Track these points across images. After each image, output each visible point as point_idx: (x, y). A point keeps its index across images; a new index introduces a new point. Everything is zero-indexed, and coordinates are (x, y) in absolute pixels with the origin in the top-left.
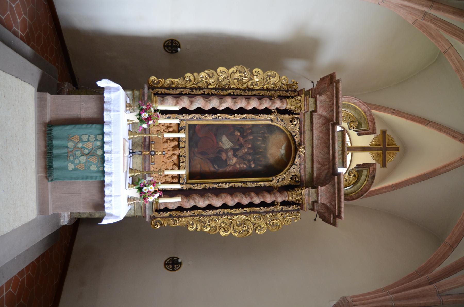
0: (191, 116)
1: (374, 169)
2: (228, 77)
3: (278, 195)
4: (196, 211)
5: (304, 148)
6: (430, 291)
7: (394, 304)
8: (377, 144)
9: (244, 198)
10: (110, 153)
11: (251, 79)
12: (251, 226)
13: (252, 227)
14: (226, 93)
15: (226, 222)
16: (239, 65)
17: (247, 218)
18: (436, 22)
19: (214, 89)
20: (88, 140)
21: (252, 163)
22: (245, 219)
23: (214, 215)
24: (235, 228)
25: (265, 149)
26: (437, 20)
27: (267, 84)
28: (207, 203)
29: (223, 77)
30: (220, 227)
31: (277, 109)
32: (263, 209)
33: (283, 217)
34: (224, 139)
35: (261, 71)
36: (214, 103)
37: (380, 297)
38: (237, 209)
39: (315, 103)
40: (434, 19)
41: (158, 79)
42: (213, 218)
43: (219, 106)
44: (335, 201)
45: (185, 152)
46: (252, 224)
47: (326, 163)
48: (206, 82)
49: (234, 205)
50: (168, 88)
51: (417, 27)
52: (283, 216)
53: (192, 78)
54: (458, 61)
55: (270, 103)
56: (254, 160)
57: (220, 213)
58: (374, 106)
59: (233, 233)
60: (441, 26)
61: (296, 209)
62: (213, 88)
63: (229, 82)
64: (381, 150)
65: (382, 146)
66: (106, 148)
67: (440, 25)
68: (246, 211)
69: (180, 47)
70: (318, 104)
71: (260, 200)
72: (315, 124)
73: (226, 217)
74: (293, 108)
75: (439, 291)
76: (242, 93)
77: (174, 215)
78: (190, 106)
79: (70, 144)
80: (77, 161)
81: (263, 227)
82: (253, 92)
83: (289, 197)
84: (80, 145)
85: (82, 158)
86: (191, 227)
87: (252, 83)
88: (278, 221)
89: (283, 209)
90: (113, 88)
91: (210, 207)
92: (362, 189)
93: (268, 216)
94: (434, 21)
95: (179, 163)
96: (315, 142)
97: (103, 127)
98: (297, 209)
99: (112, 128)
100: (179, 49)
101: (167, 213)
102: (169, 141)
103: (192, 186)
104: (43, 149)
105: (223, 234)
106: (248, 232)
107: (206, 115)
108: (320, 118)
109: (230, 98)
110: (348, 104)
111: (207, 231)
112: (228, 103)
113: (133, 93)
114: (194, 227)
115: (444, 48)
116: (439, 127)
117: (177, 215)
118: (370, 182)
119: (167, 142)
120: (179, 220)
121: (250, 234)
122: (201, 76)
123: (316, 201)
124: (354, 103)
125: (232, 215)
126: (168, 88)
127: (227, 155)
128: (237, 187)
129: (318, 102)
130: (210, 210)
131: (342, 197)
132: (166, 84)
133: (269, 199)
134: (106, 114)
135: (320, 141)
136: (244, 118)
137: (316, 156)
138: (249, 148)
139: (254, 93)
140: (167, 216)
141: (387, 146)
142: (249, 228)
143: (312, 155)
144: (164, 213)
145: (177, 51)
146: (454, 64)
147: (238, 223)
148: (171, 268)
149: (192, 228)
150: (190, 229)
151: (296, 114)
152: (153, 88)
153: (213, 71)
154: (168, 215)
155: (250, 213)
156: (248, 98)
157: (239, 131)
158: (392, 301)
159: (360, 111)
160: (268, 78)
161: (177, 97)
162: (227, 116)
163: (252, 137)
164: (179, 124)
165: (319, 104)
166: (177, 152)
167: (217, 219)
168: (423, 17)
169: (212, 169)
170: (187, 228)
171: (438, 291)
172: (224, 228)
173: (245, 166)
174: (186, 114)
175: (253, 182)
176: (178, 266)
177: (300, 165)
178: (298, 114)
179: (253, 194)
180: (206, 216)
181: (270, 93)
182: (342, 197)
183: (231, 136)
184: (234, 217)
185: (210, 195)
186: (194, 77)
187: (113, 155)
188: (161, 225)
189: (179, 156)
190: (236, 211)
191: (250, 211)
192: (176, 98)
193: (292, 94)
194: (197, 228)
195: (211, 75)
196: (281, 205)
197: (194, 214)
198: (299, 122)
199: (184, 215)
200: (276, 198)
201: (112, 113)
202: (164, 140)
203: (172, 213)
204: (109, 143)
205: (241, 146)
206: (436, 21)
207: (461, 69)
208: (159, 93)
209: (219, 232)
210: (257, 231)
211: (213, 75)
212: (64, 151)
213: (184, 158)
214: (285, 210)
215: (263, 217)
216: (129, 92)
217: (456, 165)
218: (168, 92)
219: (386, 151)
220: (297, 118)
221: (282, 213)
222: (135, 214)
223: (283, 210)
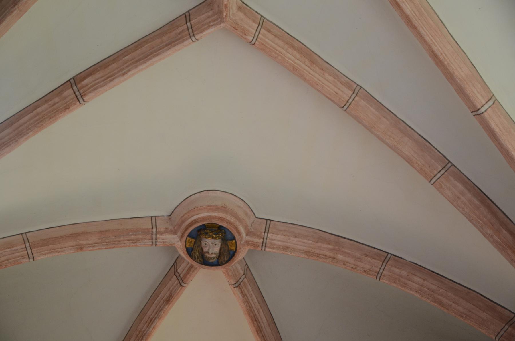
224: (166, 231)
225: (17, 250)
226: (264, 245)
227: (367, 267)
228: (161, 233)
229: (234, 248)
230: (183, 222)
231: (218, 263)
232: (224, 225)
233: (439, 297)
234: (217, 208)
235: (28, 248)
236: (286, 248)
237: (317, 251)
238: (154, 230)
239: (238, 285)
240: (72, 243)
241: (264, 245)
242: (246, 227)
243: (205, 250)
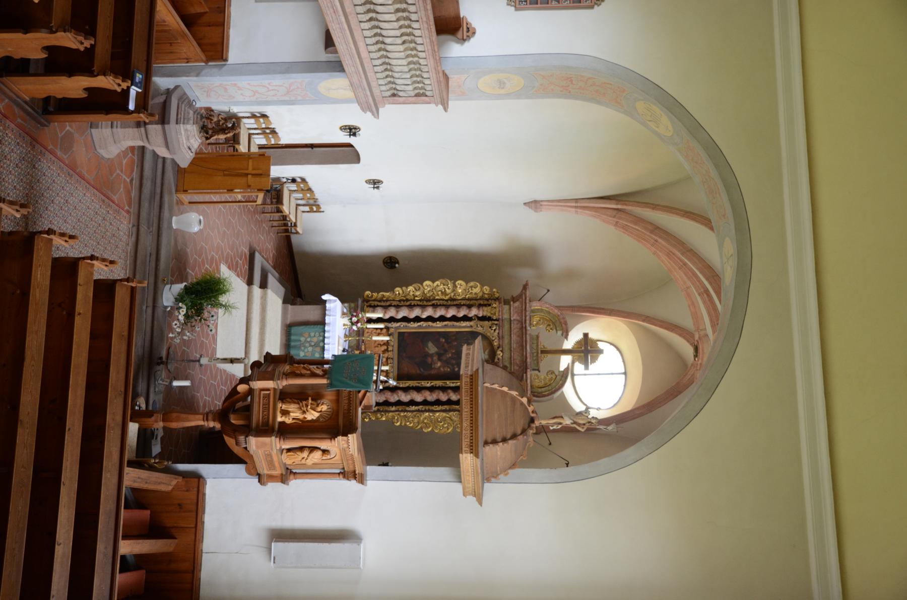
0: (399, 324)
2: (433, 289)
5: (502, 351)
10: (329, 344)
11: (454, 291)
14: (430, 304)
16: (443, 278)
19: (419, 300)
20: (315, 336)
21: (455, 366)
22: (446, 417)
27: (470, 294)
29: (429, 289)
34: (430, 345)
35: (463, 283)
36: (416, 312)
39: (510, 309)
41: (372, 293)
47: (522, 365)
49: (433, 400)
50: (380, 301)
53: (401, 292)
55: (468, 311)
63: (434, 294)
66: (326, 341)
69: (398, 263)
70: (512, 310)
73: (427, 414)
74: (489, 315)
76: (445, 303)
78: (396, 315)
79: (302, 339)
80: (306, 350)
82: (454, 302)
84: (309, 340)
85: (309, 348)
87: (455, 294)
97: (325, 326)
99: (331, 328)
100: (397, 265)
102: (379, 346)
104: (284, 341)
105: (425, 431)
106: (448, 429)
107: (412, 323)
108: (517, 324)
110: (541, 309)
112: (429, 312)
113: (350, 305)
119: (378, 347)
122: (409, 290)
124: (547, 308)
128: (437, 386)
129: (512, 308)
132: (379, 297)
134: (327, 318)
135: (518, 345)
136: (445, 325)
138: (453, 353)
139: (455, 303)
143: (511, 358)
145: (395, 267)
149: (397, 422)
152: (368, 301)
153: (419, 285)
155: (450, 411)
157: (444, 337)
160: (470, 289)
162: (430, 323)
163: (456, 343)
165: (513, 310)
166: (386, 355)
169: (418, 372)
170: (393, 423)
173: (449, 370)
174: (394, 322)
179: (450, 391)
180: (410, 411)
185: (411, 391)
186: (403, 291)
187: (330, 346)
192: (385, 308)
195: (417, 288)
198: (498, 328)
201: (331, 317)
202: (376, 345)
204: (329, 338)
205: (446, 351)
208: (372, 305)
211: (420, 288)
212: (298, 343)
213: (391, 360)
216: (346, 305)
218: (379, 304)
220: (496, 324)
224: (699, 335)
234: (703, 350)
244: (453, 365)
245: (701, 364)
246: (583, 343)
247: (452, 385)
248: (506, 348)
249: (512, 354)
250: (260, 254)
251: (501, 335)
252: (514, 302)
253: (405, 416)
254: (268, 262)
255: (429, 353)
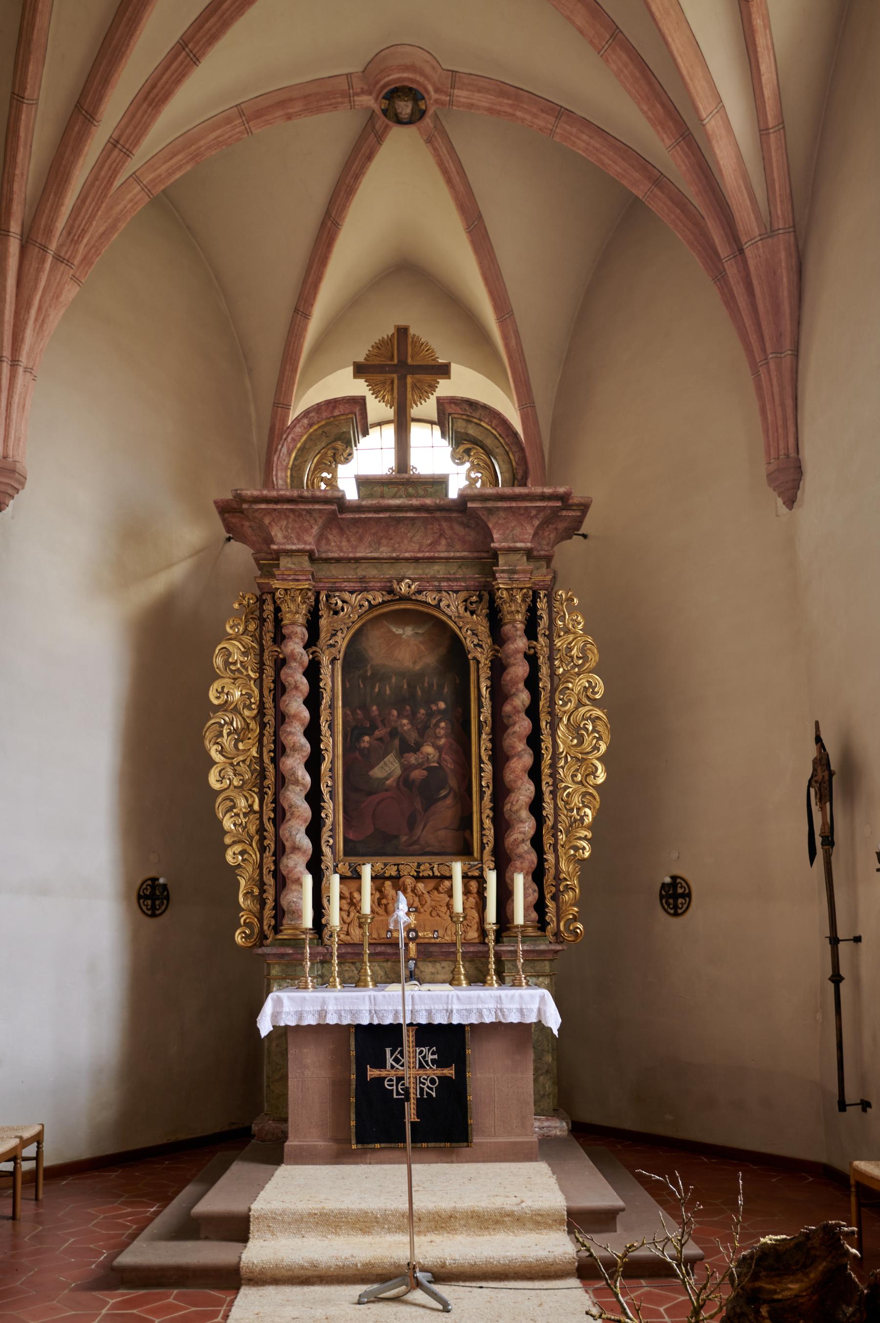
0: (326, 850)
1: (451, 403)
2: (232, 764)
3: (511, 647)
4: (544, 838)
5: (400, 581)
6: (760, 256)
7: (789, 352)
8: (390, 388)
9: (517, 728)
11: (236, 710)
12: (584, 711)
13: (587, 708)
14: (271, 768)
15: (573, 769)
17: (565, 720)
18: (77, 231)
19: (262, 797)
21: (434, 707)
22: (567, 726)
23: (554, 799)
24: (589, 749)
25: (402, 674)
26: (72, 227)
27: (247, 669)
28: (525, 814)
30: (583, 785)
31: (305, 647)
32: (544, 683)
33: (565, 633)
35: (217, 685)
37: (771, 385)
38: (542, 744)
40: (69, 233)
42: (563, 800)
43: (304, 785)
44: (527, 508)
45: (409, 865)
46: (580, 709)
47: (436, 526)
48: (246, 815)
49: (531, 752)
50: (263, 903)
51: (87, 272)
52: (562, 634)
53: (238, 848)
54: (171, 159)
56: (429, 701)
57: (550, 784)
58: (288, 367)
59: (599, 754)
60: (87, 216)
61: (547, 602)
62: (259, 800)
63: (244, 761)
64: (405, 378)
65: (395, 376)
67: (86, 218)
68: (547, 723)
71: (522, 692)
72: (341, 551)
73: (561, 771)
75: (760, 235)
76: (269, 730)
77: (553, 889)
81: (588, 682)
82: (267, 706)
83: (515, 621)
86: (581, 851)
87: (245, 706)
88: (574, 646)
89: (544, 634)
90: (274, 1006)
91: (536, 807)
92: (500, 436)
93: (561, 670)
94: (75, 235)
95: (434, 877)
96: (384, 552)
98: (545, 600)
101: (548, 906)
102: (384, 901)
103: (488, 849)
105: (601, 777)
106: (598, 718)
107: (323, 815)
108: (328, 541)
109: (283, 759)
111: (592, 815)
114: (581, 844)
115: (139, 197)
116: (342, 193)
117: (554, 884)
118: (483, 414)
119: (386, 906)
120: (565, 880)
121: (604, 713)
122: (233, 827)
123: (529, 554)
125: (555, 757)
126: (263, 903)
127: (415, 767)
128: (489, 745)
130: (543, 808)
131: (518, 490)
132: (252, 906)
133: (520, 670)
135: (384, 541)
137: (420, 551)
139: (269, 703)
140: (554, 905)
141: (396, 361)
142: (588, 715)
143: (416, 560)
144: (547, 913)
146: (179, 168)
147: (575, 741)
148: (684, 902)
149: (584, 848)
150: (587, 854)
151: (317, 601)
152: (263, 936)
153: (219, 800)
154: (553, 902)
155: (552, 713)
156: (282, 718)
158: (783, 355)
159: (309, 438)
160: (233, 668)
161: (282, 881)
162: (325, 766)
163: (375, 708)
164: (343, 878)
166: (409, 881)
167: (565, 790)
168: (67, 264)
169: (449, 801)
170: (584, 860)
171: (759, 238)
172: (587, 775)
173: (443, 724)
174: (321, 861)
175: (480, 705)
176: (679, 885)
177: (440, 591)
178: (318, 594)
179: (507, 708)
180: (556, 815)
181: (269, 663)
182: (518, 490)
183: (371, 758)
184: (561, 750)
185: (508, 807)
186: (234, 843)
188: (575, 919)
189: (418, 878)
190: (546, 747)
191: (549, 713)
193: (269, 608)
194: (585, 838)
195: (229, 803)
196: (536, 640)
197: (551, 844)
199: (553, 868)
200: (517, 651)
202: (381, 911)
203: (548, 894)
205: (394, 733)
206: (74, 231)
207: (194, 147)
208: (273, 922)
209: (596, 787)
210: (598, 697)
211: (227, 798)
213: (422, 867)
214: (548, 629)
215: (564, 683)
217: (443, 151)
218: (270, 904)
219: (407, 363)
220: (328, 597)
221: (555, 634)
222: (547, 976)
223: (547, 633)
224: (363, 92)
225: (235, 125)
226: (451, 103)
227: (542, 124)
228: (357, 94)
229: (423, 107)
230: (377, 83)
231: (410, 122)
232: (414, 86)
233: (602, 156)
235: (245, 122)
236: (471, 106)
237: (499, 108)
238: (351, 91)
239: (429, 141)
240: (280, 113)
241: (451, 103)
242: (434, 85)
243: (399, 111)
244: (430, 714)
245: (437, 90)
246: (380, 377)
247: (487, 711)
248: (391, 572)
249: (407, 555)
250: (127, 1245)
251: (357, 586)
252: (273, 542)
253: (568, 832)
254: (150, 1220)
255: (401, 776)
